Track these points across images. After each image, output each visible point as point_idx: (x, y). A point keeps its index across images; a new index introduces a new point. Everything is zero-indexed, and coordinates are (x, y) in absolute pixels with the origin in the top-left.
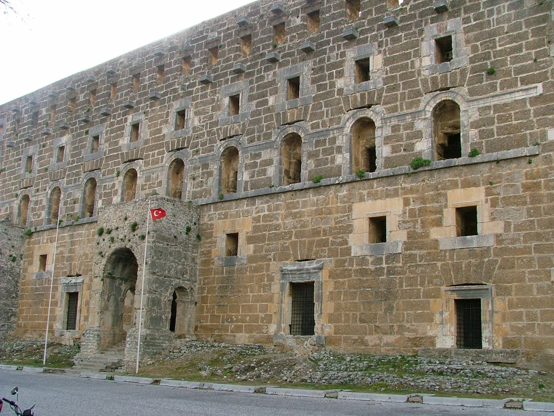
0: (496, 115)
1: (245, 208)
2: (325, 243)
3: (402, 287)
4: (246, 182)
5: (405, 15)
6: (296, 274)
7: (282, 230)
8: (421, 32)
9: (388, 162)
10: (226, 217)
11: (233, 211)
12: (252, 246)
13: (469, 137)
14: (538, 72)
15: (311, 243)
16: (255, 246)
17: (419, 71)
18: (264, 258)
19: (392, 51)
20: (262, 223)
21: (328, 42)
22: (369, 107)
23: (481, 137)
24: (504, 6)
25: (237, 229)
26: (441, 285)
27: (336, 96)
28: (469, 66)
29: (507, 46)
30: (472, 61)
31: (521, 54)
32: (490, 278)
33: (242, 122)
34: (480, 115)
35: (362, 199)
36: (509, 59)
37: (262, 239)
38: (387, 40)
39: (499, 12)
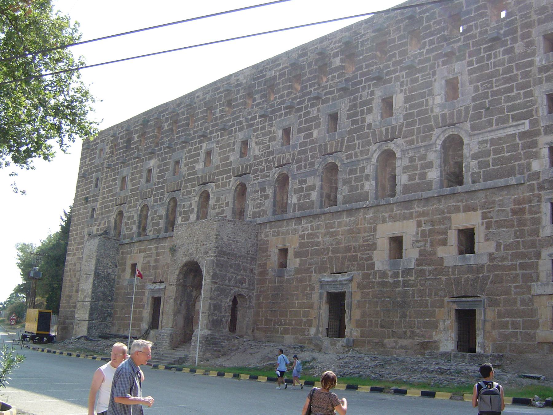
0: (492, 148)
1: (294, 227)
2: (355, 258)
3: (414, 297)
4: (295, 205)
5: (422, 58)
6: (331, 285)
7: (321, 247)
8: (434, 74)
9: (406, 189)
10: (278, 235)
11: (284, 229)
12: (298, 260)
13: (471, 166)
14: (525, 110)
15: (344, 258)
16: (300, 260)
17: (432, 108)
18: (307, 270)
19: (411, 90)
20: (306, 240)
21: (360, 82)
22: (392, 140)
23: (480, 168)
24: (499, 51)
25: (287, 245)
26: (445, 297)
27: (366, 131)
28: (472, 105)
29: (502, 87)
30: (474, 99)
31: (513, 94)
33: (292, 152)
34: (479, 148)
35: (384, 221)
36: (503, 98)
37: (306, 254)
38: (407, 81)
39: (496, 56)
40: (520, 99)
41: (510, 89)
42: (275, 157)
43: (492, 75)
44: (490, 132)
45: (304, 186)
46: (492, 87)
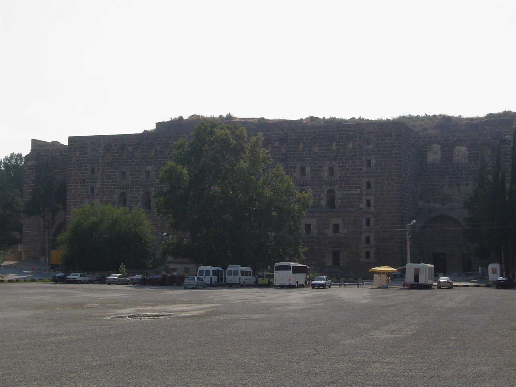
13: (338, 202)
30: (340, 177)
41: (354, 177)
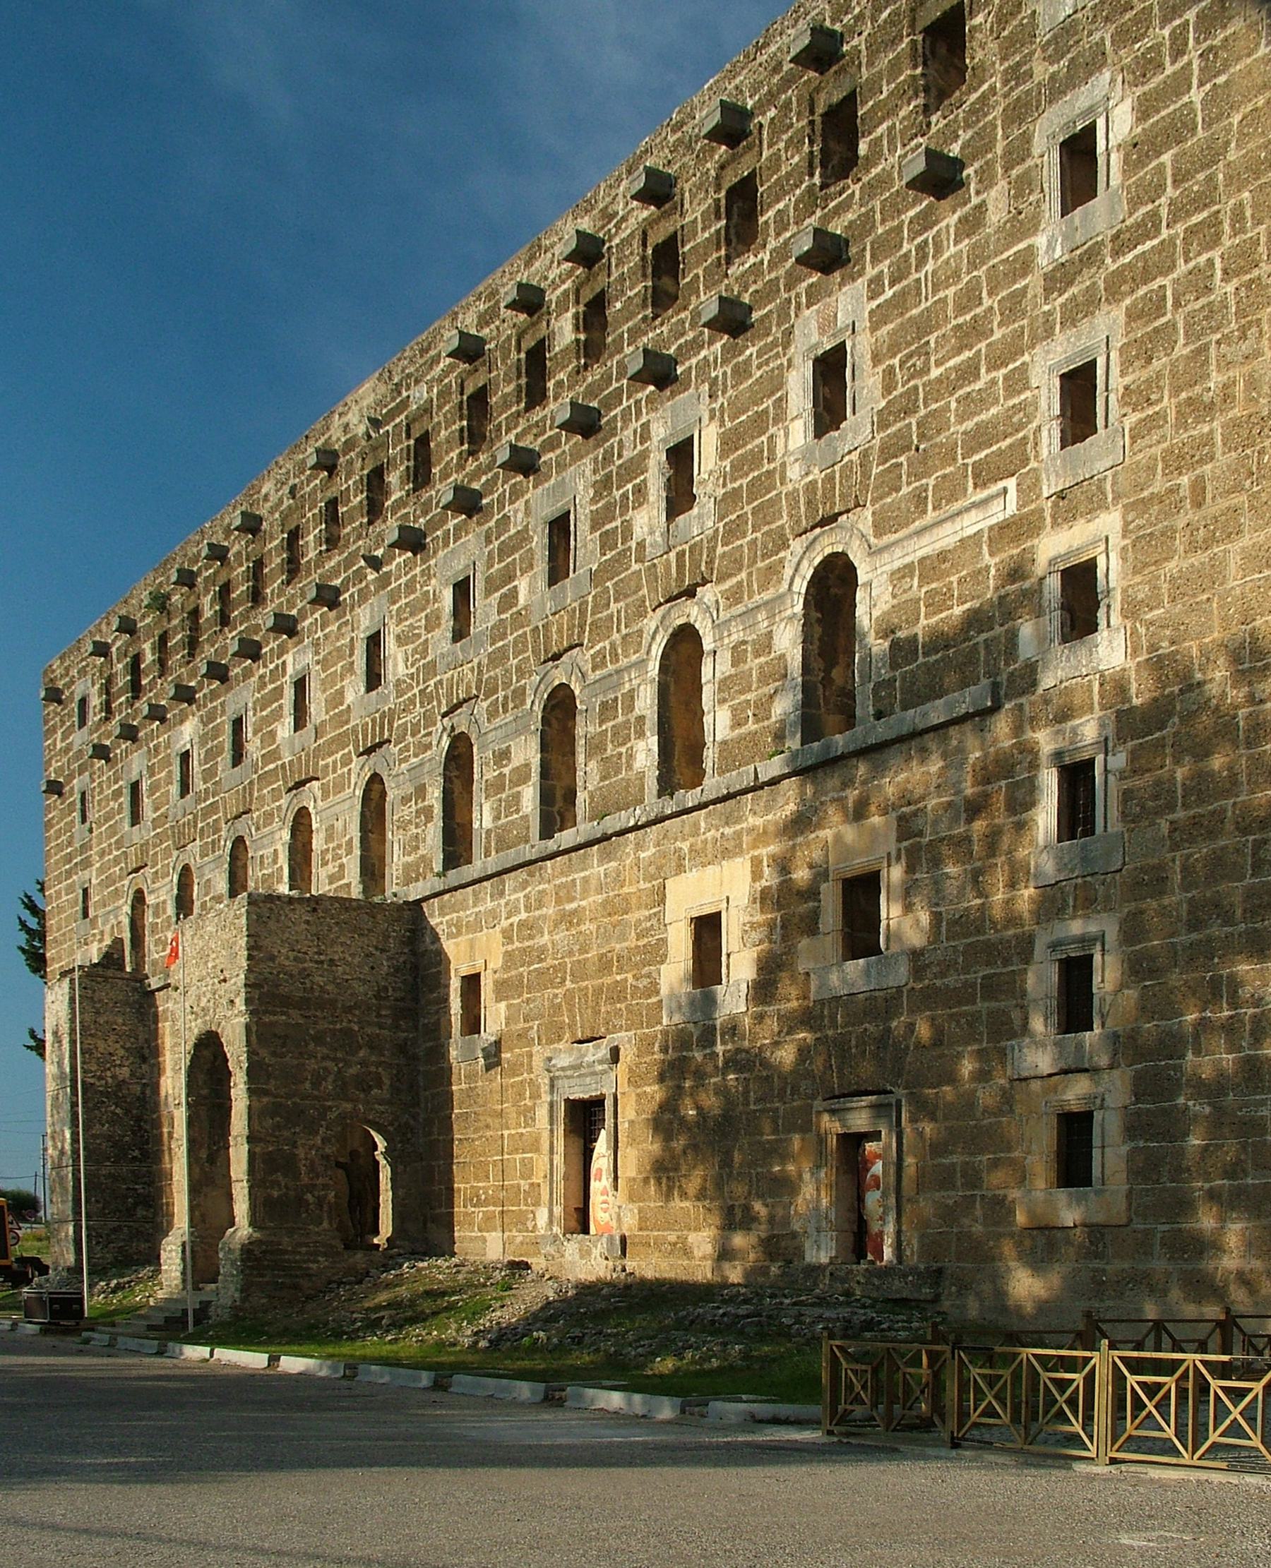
0: (924, 590)
3: (748, 1104)
4: (488, 832)
6: (572, 1077)
7: (550, 962)
9: (731, 755)
10: (459, 933)
11: (468, 914)
12: (503, 1005)
16: (508, 1007)
20: (517, 944)
22: (690, 593)
24: (948, 226)
26: (813, 1097)
28: (877, 442)
29: (951, 363)
31: (978, 385)
32: (900, 1075)
33: (476, 661)
34: (894, 597)
35: (680, 869)
36: (953, 405)
39: (938, 250)
40: (996, 401)
41: (969, 372)
42: (440, 682)
43: (923, 326)
44: (919, 533)
45: (506, 771)
46: (926, 370)
